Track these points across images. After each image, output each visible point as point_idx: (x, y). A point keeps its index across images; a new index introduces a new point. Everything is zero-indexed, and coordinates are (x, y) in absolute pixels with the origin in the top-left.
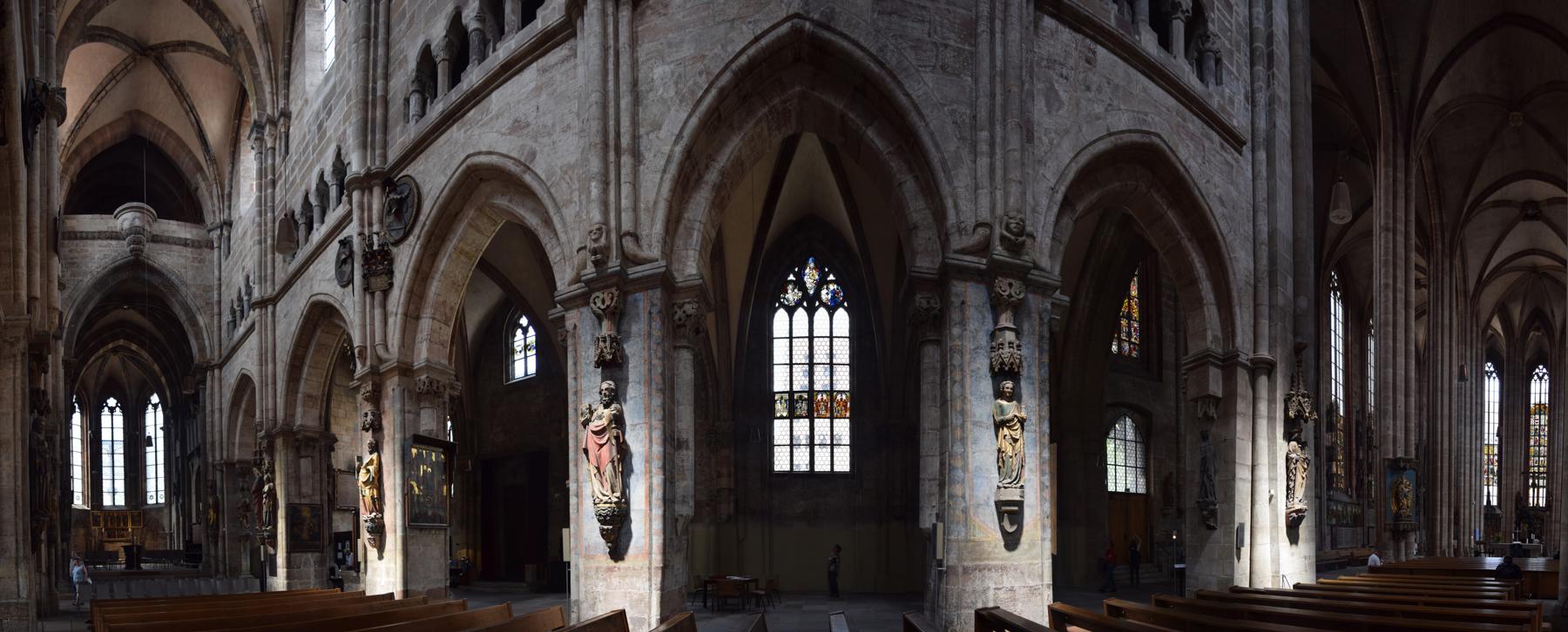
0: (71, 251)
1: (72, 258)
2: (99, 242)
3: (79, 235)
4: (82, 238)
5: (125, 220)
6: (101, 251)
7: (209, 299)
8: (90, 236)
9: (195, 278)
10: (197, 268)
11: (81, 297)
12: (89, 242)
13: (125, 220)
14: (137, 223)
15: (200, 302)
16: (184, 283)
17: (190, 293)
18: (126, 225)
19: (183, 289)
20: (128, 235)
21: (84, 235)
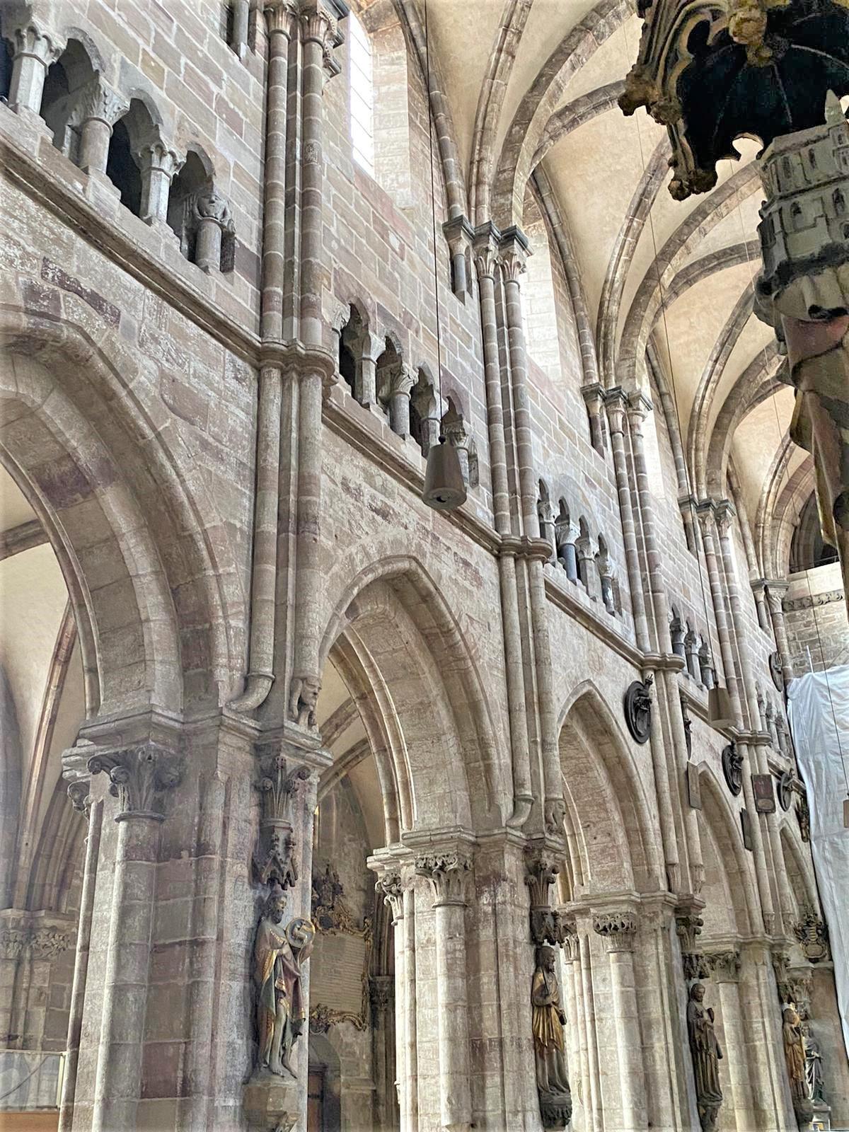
0: (808, 625)
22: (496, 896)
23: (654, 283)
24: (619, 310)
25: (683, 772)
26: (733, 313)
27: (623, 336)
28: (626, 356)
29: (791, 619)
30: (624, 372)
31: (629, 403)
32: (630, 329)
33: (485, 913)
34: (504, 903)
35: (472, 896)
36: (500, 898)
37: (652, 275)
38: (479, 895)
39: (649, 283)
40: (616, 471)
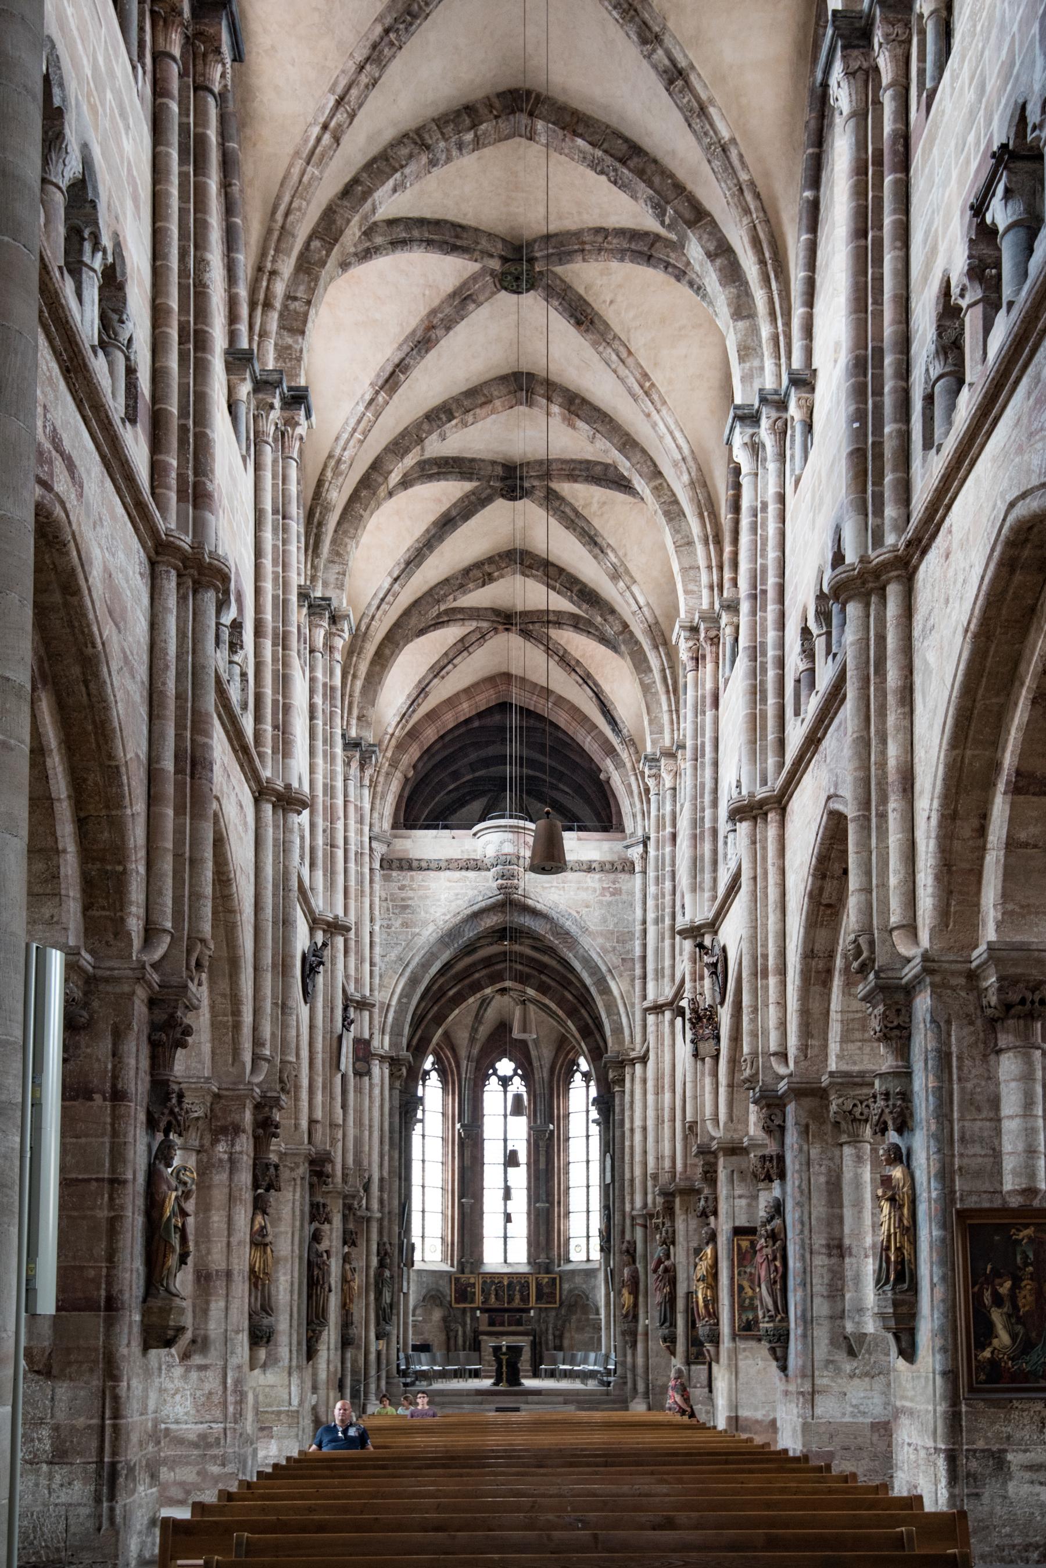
1: (403, 899)
2: (448, 873)
3: (415, 864)
4: (420, 869)
5: (488, 843)
6: (449, 888)
7: (628, 952)
8: (433, 865)
9: (604, 920)
10: (610, 904)
11: (417, 959)
12: (432, 874)
13: (488, 843)
14: (508, 849)
15: (614, 960)
16: (585, 930)
17: (593, 945)
18: (491, 852)
19: (586, 942)
20: (493, 866)
21: (424, 865)
22: (233, 1145)
23: (380, 479)
24: (338, 496)
25: (335, 1036)
26: (428, 531)
27: (335, 531)
28: (336, 559)
29: (387, 878)
30: (332, 578)
31: (334, 620)
32: (346, 525)
33: (221, 1160)
34: (241, 1153)
35: (207, 1142)
36: (238, 1148)
37: (377, 466)
38: (215, 1142)
39: (374, 476)
40: (311, 698)
